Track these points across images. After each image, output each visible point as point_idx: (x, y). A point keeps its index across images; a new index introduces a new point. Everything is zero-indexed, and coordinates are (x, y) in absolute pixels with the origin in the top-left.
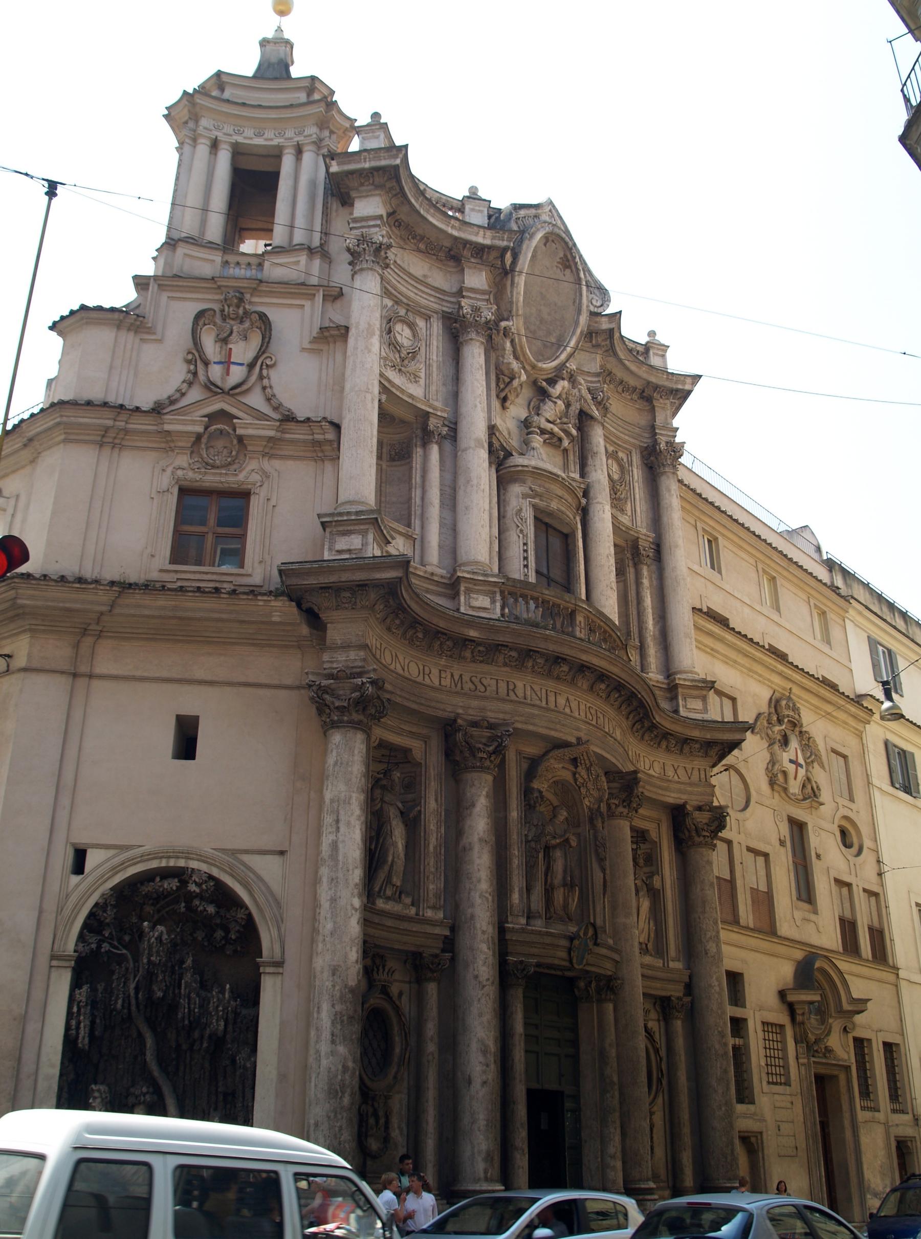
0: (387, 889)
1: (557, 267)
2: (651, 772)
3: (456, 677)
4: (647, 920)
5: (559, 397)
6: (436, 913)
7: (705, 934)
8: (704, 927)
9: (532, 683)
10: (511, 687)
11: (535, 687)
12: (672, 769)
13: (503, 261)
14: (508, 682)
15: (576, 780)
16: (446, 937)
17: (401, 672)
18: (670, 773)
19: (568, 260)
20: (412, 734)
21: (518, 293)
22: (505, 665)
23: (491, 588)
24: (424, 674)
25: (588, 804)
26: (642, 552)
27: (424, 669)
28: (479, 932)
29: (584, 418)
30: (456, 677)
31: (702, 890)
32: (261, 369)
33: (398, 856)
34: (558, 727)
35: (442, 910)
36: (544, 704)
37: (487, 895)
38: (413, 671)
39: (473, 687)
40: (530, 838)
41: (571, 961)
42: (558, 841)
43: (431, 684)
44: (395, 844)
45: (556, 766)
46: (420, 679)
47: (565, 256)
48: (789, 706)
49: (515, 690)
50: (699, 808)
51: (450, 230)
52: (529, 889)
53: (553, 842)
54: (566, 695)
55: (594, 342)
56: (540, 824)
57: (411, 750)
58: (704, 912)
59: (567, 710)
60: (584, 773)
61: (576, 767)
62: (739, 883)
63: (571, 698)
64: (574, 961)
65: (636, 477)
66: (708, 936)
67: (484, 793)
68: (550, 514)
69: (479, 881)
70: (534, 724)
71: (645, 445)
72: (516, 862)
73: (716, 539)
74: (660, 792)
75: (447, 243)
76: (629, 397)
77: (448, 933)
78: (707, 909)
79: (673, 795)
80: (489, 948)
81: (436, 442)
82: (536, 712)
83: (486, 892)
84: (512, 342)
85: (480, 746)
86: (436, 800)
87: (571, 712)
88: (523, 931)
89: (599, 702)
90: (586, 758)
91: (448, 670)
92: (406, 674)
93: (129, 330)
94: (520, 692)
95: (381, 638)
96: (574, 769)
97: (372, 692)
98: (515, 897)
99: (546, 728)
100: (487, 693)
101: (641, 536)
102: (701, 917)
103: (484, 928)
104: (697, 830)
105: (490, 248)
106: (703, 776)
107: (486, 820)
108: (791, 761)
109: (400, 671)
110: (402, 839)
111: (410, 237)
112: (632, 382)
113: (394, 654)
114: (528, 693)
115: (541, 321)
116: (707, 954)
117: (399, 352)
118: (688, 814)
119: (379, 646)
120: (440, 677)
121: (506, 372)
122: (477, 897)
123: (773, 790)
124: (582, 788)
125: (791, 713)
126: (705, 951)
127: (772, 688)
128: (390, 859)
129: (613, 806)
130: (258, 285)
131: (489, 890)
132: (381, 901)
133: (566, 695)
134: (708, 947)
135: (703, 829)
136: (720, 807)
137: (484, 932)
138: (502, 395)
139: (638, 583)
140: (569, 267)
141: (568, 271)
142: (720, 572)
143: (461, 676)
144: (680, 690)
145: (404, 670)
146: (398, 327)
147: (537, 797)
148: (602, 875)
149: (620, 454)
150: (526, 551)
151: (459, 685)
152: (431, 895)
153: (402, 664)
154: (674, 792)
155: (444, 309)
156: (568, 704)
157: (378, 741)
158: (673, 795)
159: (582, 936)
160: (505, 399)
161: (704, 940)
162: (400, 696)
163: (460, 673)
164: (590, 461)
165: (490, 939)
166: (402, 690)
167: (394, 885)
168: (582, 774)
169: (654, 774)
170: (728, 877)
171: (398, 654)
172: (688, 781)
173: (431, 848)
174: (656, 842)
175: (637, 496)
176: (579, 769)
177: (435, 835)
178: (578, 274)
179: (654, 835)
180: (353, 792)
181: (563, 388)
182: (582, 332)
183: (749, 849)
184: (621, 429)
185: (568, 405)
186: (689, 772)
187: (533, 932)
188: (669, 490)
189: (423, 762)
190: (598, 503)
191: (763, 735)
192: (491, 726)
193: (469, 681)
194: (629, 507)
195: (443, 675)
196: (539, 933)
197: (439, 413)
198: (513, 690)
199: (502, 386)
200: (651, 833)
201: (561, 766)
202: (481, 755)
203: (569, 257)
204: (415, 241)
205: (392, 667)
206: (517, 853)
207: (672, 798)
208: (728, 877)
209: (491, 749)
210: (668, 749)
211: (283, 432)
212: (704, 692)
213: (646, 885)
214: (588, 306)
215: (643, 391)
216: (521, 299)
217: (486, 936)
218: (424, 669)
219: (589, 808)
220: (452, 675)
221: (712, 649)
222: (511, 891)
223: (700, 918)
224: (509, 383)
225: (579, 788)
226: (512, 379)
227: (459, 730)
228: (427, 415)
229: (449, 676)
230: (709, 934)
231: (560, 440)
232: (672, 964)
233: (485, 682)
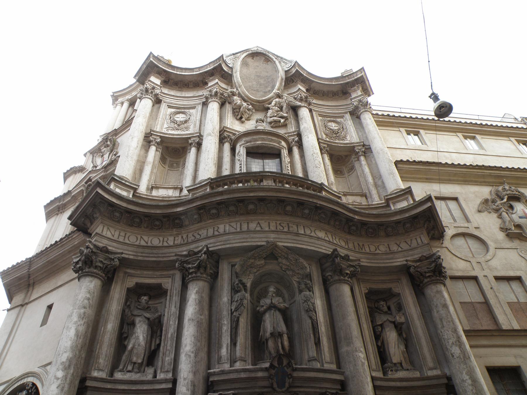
0: (129, 366)
1: (263, 64)
2: (378, 251)
3: (185, 237)
4: (397, 346)
5: (275, 105)
6: (167, 375)
7: (448, 342)
8: (446, 337)
9: (229, 222)
10: (216, 229)
11: (232, 224)
12: (396, 245)
13: (224, 71)
14: (214, 228)
15: (281, 268)
16: (171, 388)
17: (146, 244)
18: (395, 248)
19: (268, 59)
20: (161, 277)
21: (237, 79)
22: (211, 219)
23: (205, 188)
24: (163, 241)
25: (297, 280)
26: (357, 150)
27: (163, 240)
28: (182, 380)
29: (295, 109)
30: (185, 237)
31: (438, 312)
32: (112, 156)
33: (139, 345)
34: (249, 240)
35: (172, 372)
36: (238, 230)
37: (189, 354)
38: (156, 242)
39: (193, 238)
40: (233, 310)
41: (272, 386)
42: (265, 308)
43: (168, 245)
44: (138, 338)
45: (258, 263)
46: (161, 245)
47: (265, 58)
48: (505, 189)
49: (219, 230)
50: (420, 260)
51: (195, 73)
52: (234, 342)
53: (262, 309)
54: (257, 222)
55: (295, 81)
56: (239, 299)
57: (161, 284)
58: (443, 327)
59: (258, 229)
60: (284, 261)
61: (277, 259)
62: (492, 301)
63: (260, 222)
64: (275, 386)
65: (350, 124)
66: (450, 343)
67: (195, 291)
68: (258, 147)
69: (186, 346)
70: (230, 244)
71: (352, 110)
72: (225, 328)
73: (419, 132)
74: (388, 261)
75: (200, 79)
76: (338, 97)
77: (170, 386)
78: (445, 323)
79: (399, 260)
80: (188, 390)
81: (195, 146)
82: (231, 236)
83: (190, 351)
84: (240, 95)
85: (190, 266)
86: (175, 307)
87: (262, 228)
88: (223, 372)
89: (288, 218)
90: (280, 252)
91: (180, 237)
92: (149, 244)
93: (79, 173)
94: (221, 230)
95: (124, 231)
96: (275, 262)
97: (86, 253)
98: (224, 351)
99: (239, 243)
100: (202, 237)
101: (355, 145)
102: (442, 331)
103: (185, 377)
104: (422, 275)
105: (214, 69)
106: (419, 241)
107: (194, 306)
108: (520, 217)
109: (143, 243)
110: (143, 333)
111: (184, 86)
112: (335, 89)
113: (139, 237)
114: (227, 228)
115: (260, 85)
116: (453, 356)
117: (176, 123)
118: (410, 267)
119: (123, 234)
120: (174, 240)
121: (237, 107)
122: (184, 356)
123: (511, 238)
124: (287, 272)
125: (509, 192)
126: (452, 354)
127: (490, 186)
128: (130, 347)
129: (330, 277)
130: (116, 132)
131: (192, 350)
132: (120, 373)
133: (257, 222)
134: (453, 351)
135: (425, 272)
136: (434, 254)
137: (185, 379)
138: (239, 116)
139: (361, 165)
140: (270, 61)
141: (269, 63)
142: (426, 144)
143: (187, 235)
144: (391, 202)
145: (147, 243)
146: (178, 116)
147: (237, 284)
148: (310, 321)
149: (339, 120)
150: (241, 167)
151: (186, 240)
152: (166, 364)
153: (146, 240)
154: (399, 258)
155: (203, 101)
156: (258, 225)
157: (134, 283)
158: (399, 260)
159: (277, 366)
160: (241, 118)
161: (449, 347)
162: (141, 256)
163: (186, 234)
164: (300, 123)
165: (190, 382)
166: (142, 253)
167: (135, 363)
168: (284, 262)
169: (380, 252)
170: (484, 301)
171: (143, 237)
172: (410, 248)
173: (169, 335)
174: (399, 294)
175: (352, 131)
176: (280, 260)
177: (173, 327)
178: (273, 61)
179: (396, 290)
180: (75, 309)
181: (276, 102)
182: (282, 79)
183: (497, 278)
184: (335, 110)
185: (281, 108)
186: (409, 243)
187: (230, 372)
188: (365, 119)
189: (169, 289)
190: (305, 136)
191: (490, 210)
192: (196, 253)
193: (191, 236)
194: (348, 137)
195: (176, 239)
196: (237, 371)
197: (195, 135)
198: (217, 231)
199: (237, 114)
200: (393, 289)
201: (263, 262)
202: (191, 271)
203: (268, 58)
204: (187, 86)
205: (137, 243)
206: (225, 322)
207: (399, 261)
208: (484, 301)
209: (196, 265)
210: (388, 235)
211: (106, 172)
212: (407, 196)
213: (394, 323)
214: (283, 69)
215: (343, 91)
216: (240, 79)
217: (187, 381)
218: (163, 240)
219: (299, 283)
220: (182, 237)
221: (427, 179)
222: (220, 347)
223: (442, 332)
224: (239, 111)
225: (285, 271)
226: (240, 109)
227: (177, 261)
228: (190, 138)
229: (180, 237)
230: (451, 342)
231: (280, 122)
232: (430, 373)
233: (200, 233)
